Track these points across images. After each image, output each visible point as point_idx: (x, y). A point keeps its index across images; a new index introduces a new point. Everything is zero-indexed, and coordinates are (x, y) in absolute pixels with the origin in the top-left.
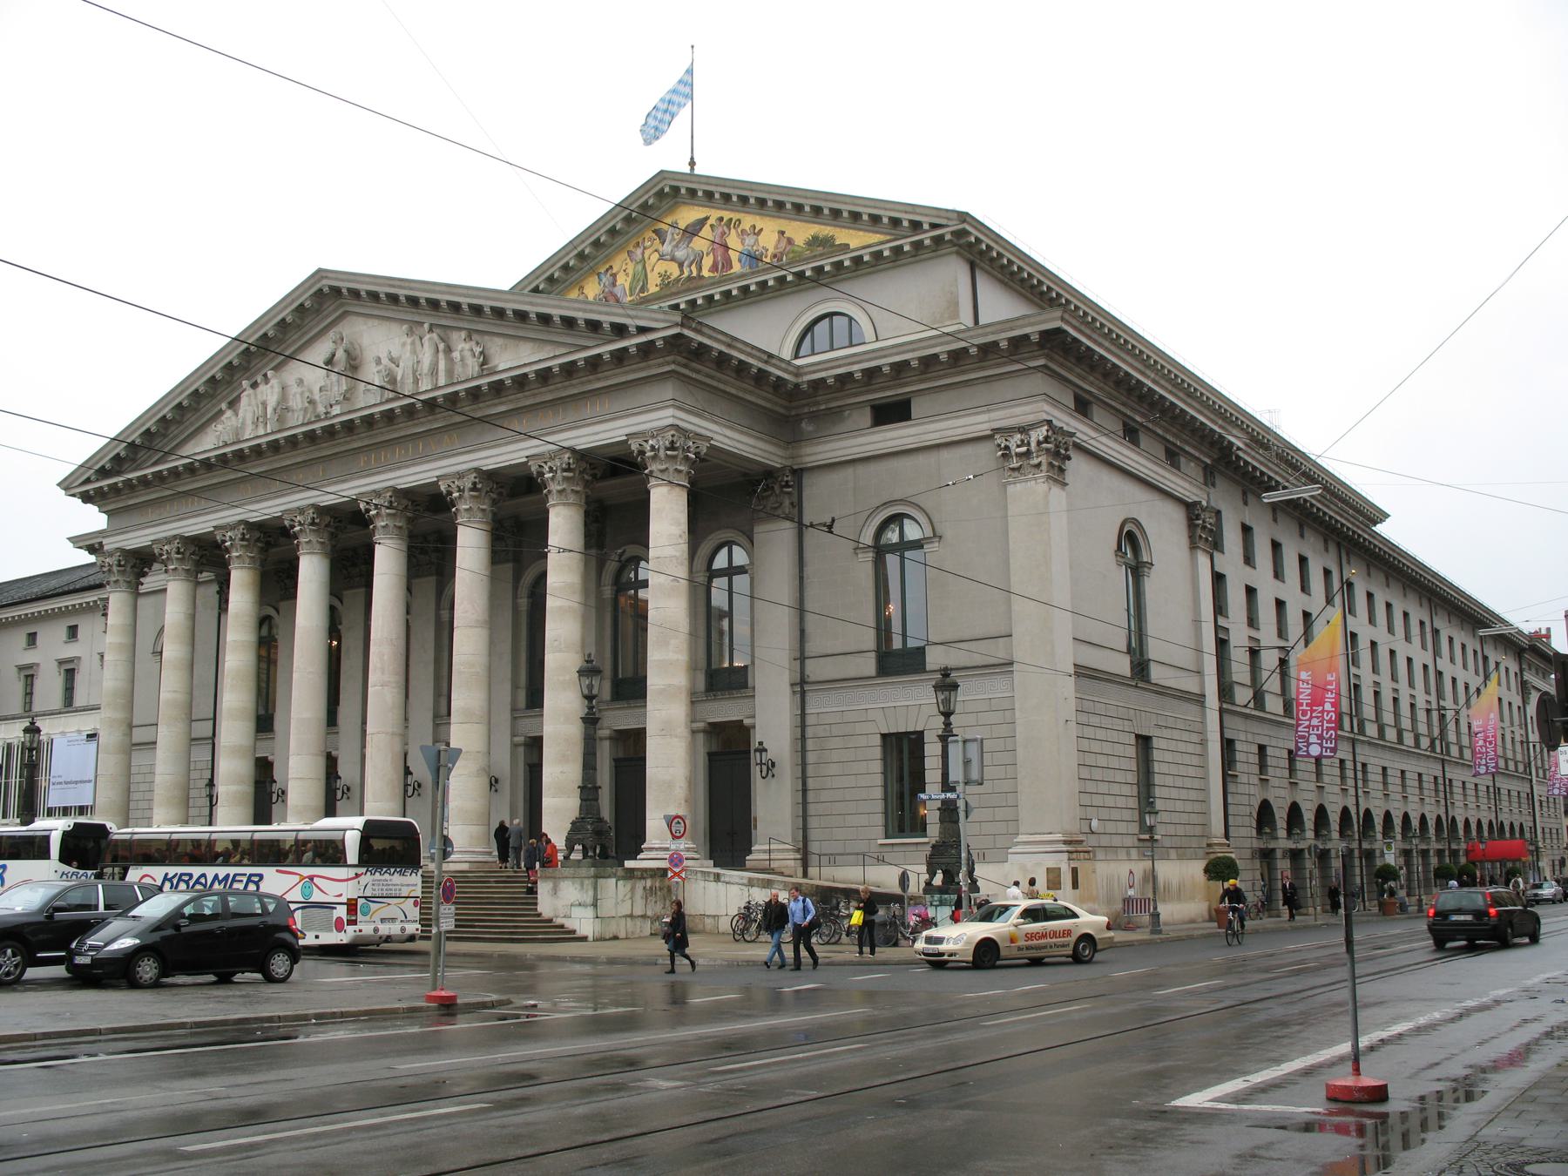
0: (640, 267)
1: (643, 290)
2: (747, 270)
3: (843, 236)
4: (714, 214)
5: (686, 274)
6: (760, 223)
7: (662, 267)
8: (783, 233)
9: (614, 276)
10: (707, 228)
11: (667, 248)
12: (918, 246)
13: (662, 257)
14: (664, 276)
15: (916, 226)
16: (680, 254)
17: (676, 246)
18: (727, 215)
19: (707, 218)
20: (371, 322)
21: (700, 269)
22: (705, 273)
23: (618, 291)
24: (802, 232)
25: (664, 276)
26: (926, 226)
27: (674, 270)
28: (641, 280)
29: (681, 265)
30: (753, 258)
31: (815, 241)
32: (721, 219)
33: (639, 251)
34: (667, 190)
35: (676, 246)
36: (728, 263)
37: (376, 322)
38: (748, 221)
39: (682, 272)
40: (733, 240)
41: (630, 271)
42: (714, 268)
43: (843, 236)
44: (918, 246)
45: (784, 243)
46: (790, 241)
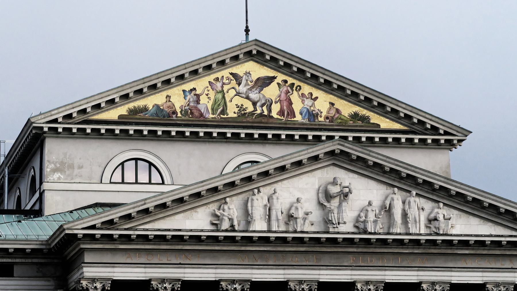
0: (220, 96)
1: (223, 112)
2: (306, 121)
3: (375, 118)
4: (280, 77)
5: (259, 111)
6: (316, 93)
7: (238, 101)
8: (332, 104)
9: (198, 96)
10: (274, 84)
11: (242, 89)
12: (436, 142)
13: (238, 94)
14: (241, 108)
15: (435, 130)
16: (254, 96)
17: (250, 89)
18: (290, 80)
19: (274, 78)
20: (351, 175)
21: (270, 111)
22: (274, 114)
23: (201, 107)
24: (347, 109)
25: (241, 108)
26: (442, 132)
27: (251, 108)
28: (221, 105)
29: (254, 104)
30: (312, 115)
31: (355, 116)
32: (286, 82)
33: (219, 85)
34: (254, 52)
35: (250, 89)
36: (292, 113)
37: (356, 176)
38: (306, 89)
39: (255, 110)
40: (295, 97)
41: (212, 98)
42: (281, 112)
43: (375, 118)
44: (436, 142)
45: (333, 112)
46: (338, 111)
